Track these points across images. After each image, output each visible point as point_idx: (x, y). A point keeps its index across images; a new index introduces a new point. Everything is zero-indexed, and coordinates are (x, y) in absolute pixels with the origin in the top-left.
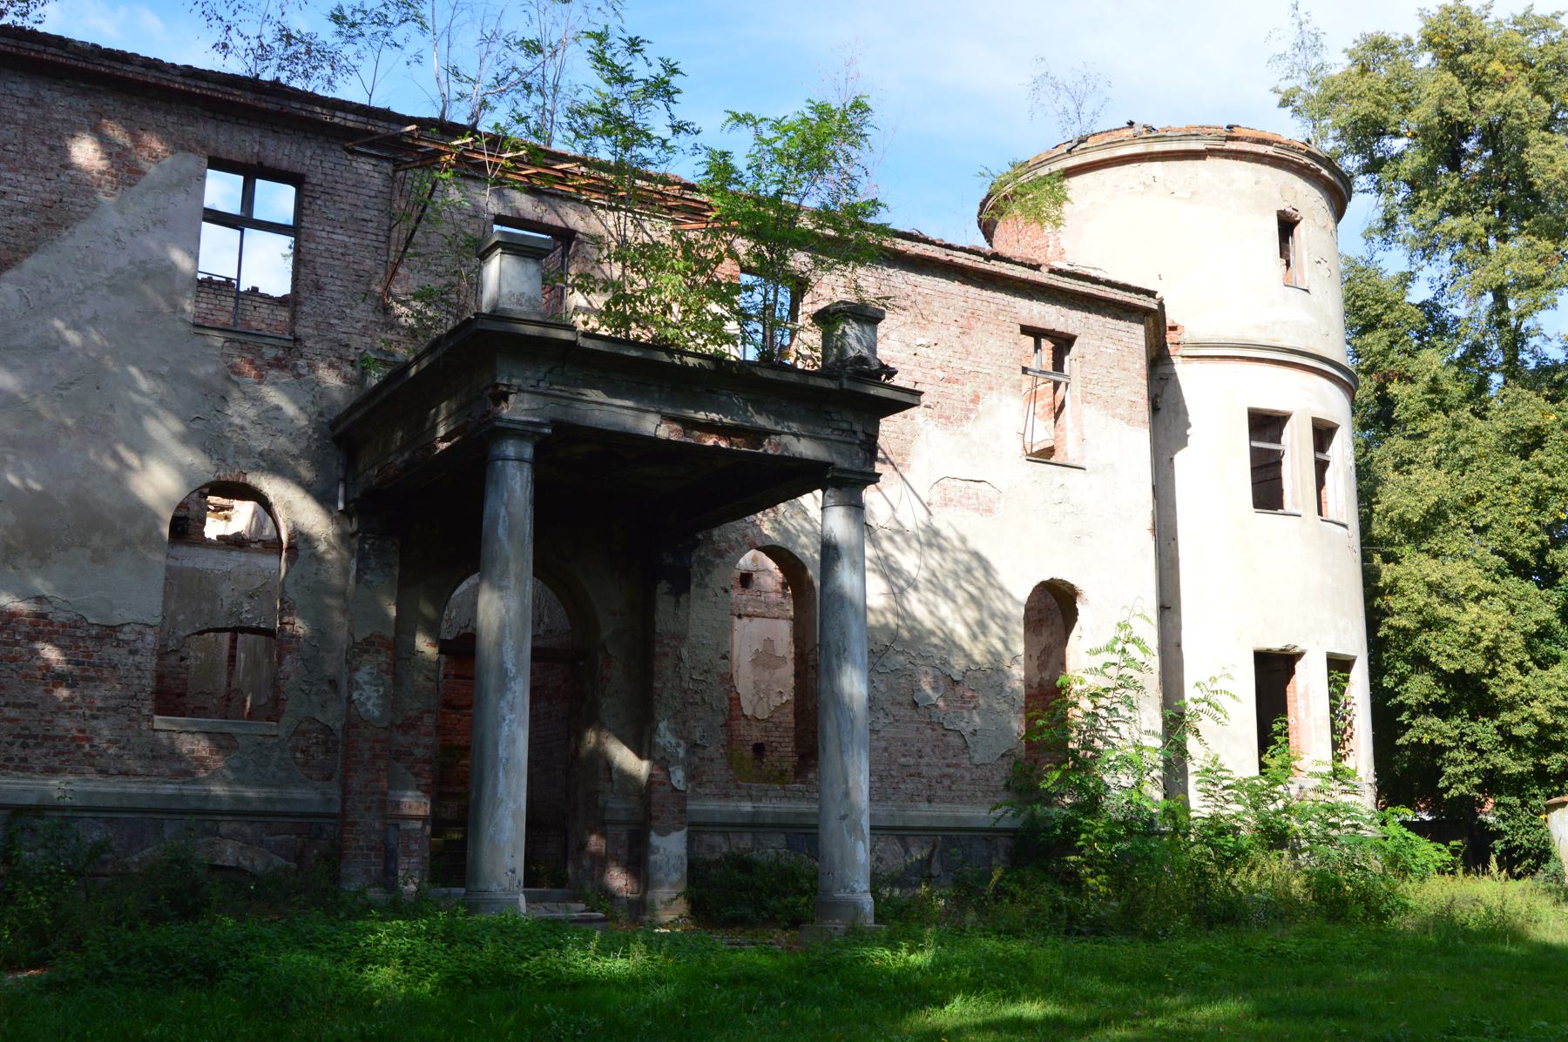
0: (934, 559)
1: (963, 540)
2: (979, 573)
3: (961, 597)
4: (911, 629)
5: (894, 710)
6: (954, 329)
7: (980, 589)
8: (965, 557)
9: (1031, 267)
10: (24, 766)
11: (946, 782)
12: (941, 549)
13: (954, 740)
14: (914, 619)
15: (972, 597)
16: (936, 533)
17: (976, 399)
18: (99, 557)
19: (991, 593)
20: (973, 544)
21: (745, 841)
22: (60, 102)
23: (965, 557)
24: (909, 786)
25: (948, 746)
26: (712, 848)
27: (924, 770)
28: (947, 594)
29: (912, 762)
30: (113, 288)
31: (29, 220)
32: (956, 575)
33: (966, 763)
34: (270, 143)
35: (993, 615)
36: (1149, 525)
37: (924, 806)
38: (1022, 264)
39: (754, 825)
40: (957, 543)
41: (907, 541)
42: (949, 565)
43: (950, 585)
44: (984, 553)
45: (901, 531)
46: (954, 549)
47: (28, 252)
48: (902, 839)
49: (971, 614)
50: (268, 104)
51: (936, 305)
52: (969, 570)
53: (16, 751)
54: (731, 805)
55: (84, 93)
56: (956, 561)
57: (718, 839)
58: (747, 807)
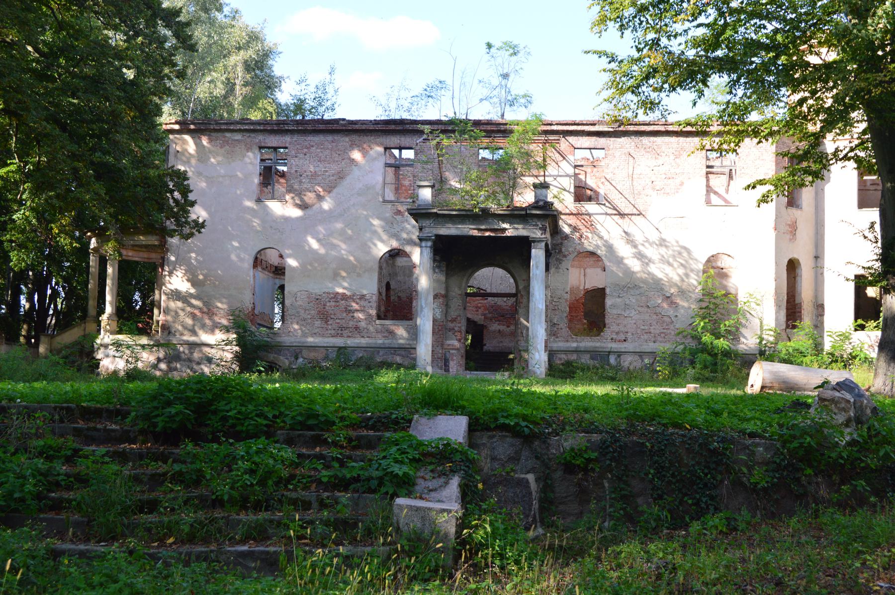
0: (663, 250)
1: (677, 242)
2: (685, 254)
3: (676, 264)
4: (653, 279)
5: (639, 309)
6: (672, 157)
7: (686, 261)
8: (678, 249)
9: (592, 125)
10: (342, 336)
11: (663, 335)
12: (666, 247)
13: (666, 319)
14: (653, 275)
15: (682, 265)
16: (664, 240)
17: (682, 184)
18: (359, 275)
19: (691, 262)
20: (681, 243)
21: (574, 357)
22: (344, 141)
23: (678, 249)
24: (646, 337)
25: (664, 322)
26: (560, 359)
27: (652, 331)
28: (670, 264)
29: (646, 328)
30: (359, 194)
31: (334, 178)
32: (674, 256)
33: (672, 327)
34: (403, 139)
35: (692, 270)
36: (772, 224)
37: (651, 344)
38: (557, 124)
39: (576, 351)
40: (675, 244)
41: (651, 244)
42: (670, 252)
43: (671, 260)
44: (687, 246)
45: (647, 241)
46: (673, 246)
47: (334, 187)
48: (641, 356)
49: (681, 271)
50: (400, 128)
51: (663, 148)
52: (680, 253)
53: (340, 332)
54: (568, 344)
55: (347, 135)
56: (674, 251)
57: (563, 356)
58: (575, 345)
